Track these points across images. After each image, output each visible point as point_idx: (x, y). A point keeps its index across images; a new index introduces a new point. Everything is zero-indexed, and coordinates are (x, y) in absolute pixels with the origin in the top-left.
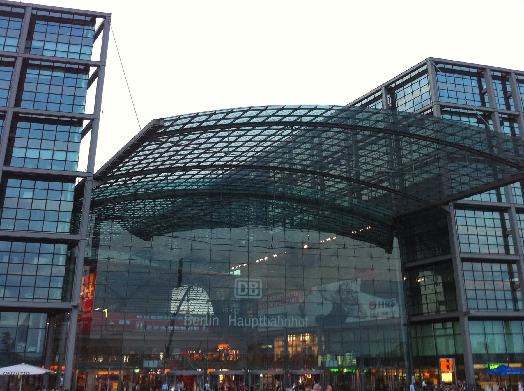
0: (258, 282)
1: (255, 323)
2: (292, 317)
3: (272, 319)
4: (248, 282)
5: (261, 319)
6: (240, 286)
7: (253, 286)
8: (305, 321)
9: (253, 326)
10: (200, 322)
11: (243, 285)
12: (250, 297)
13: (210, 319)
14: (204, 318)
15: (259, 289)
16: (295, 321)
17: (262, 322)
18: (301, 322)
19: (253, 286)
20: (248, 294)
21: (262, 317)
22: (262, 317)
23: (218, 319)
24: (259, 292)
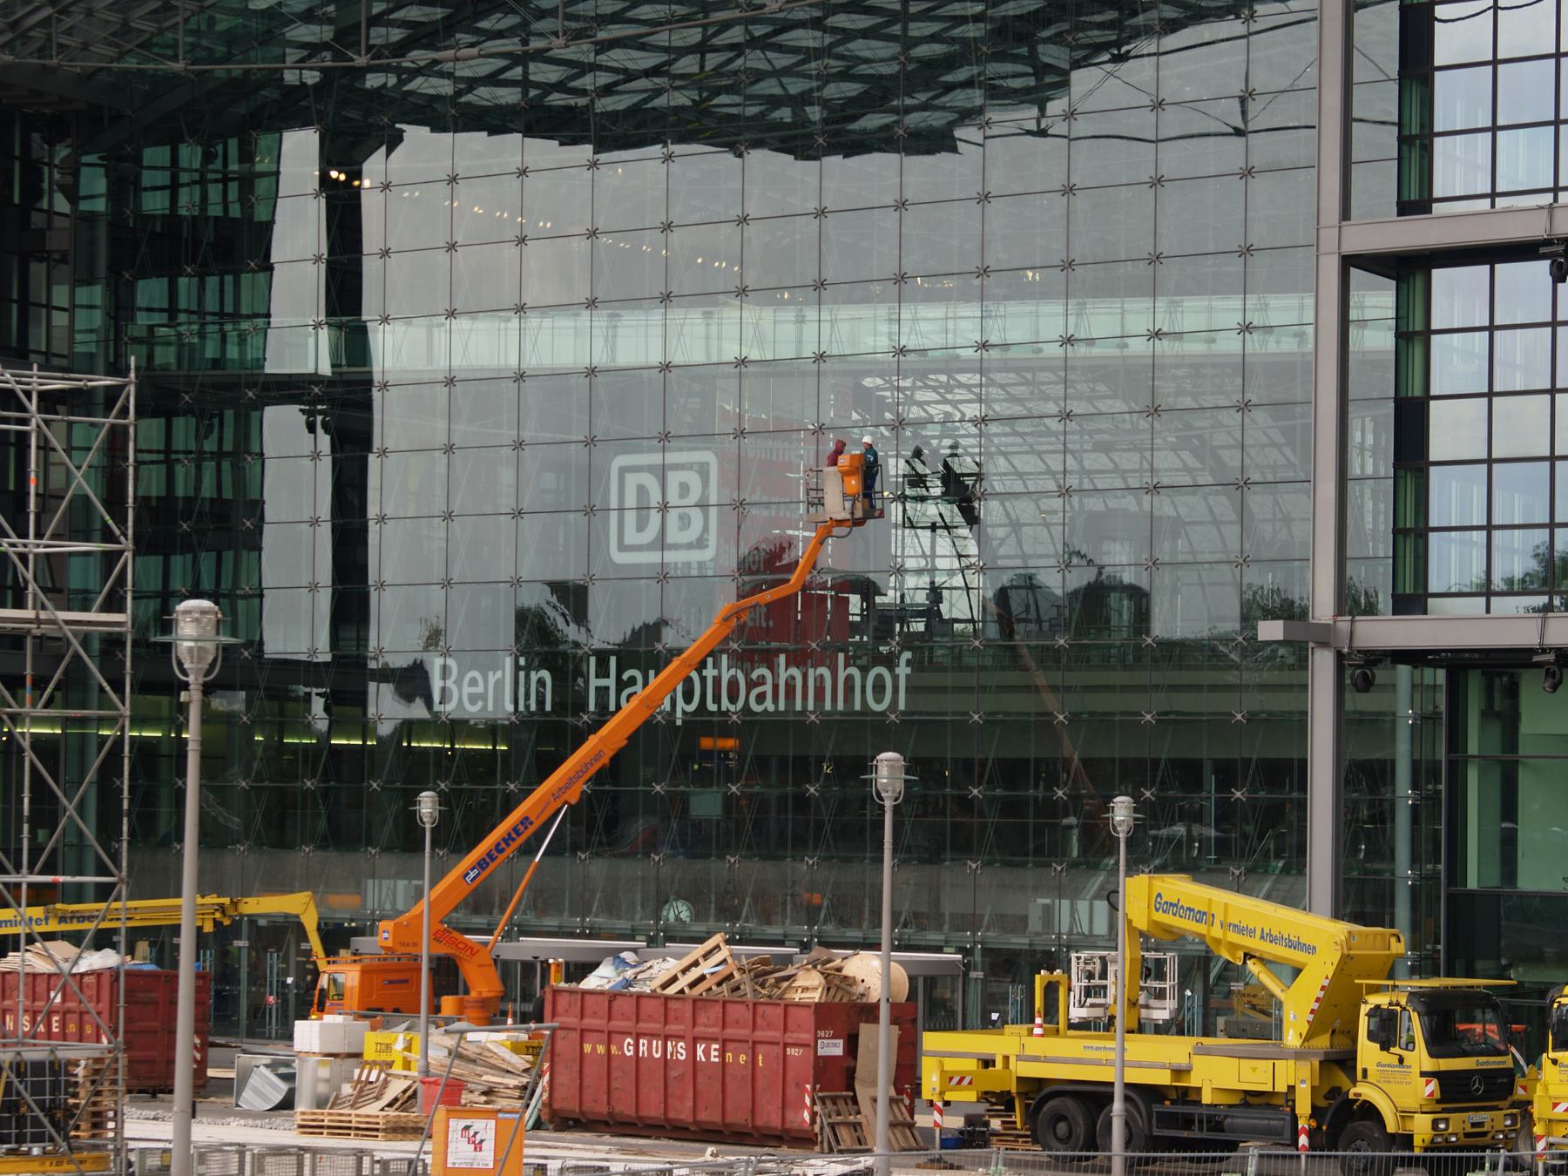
0: (703, 470)
1: (688, 700)
2: (841, 656)
3: (754, 676)
4: (662, 472)
5: (710, 672)
6: (631, 500)
7: (684, 489)
8: (895, 679)
9: (679, 714)
10: (484, 697)
11: (642, 490)
12: (671, 557)
13: (522, 674)
14: (499, 674)
15: (703, 506)
16: (849, 680)
17: (717, 681)
18: (879, 679)
19: (684, 489)
20: (661, 543)
21: (716, 665)
22: (716, 665)
23: (546, 674)
24: (706, 529)
